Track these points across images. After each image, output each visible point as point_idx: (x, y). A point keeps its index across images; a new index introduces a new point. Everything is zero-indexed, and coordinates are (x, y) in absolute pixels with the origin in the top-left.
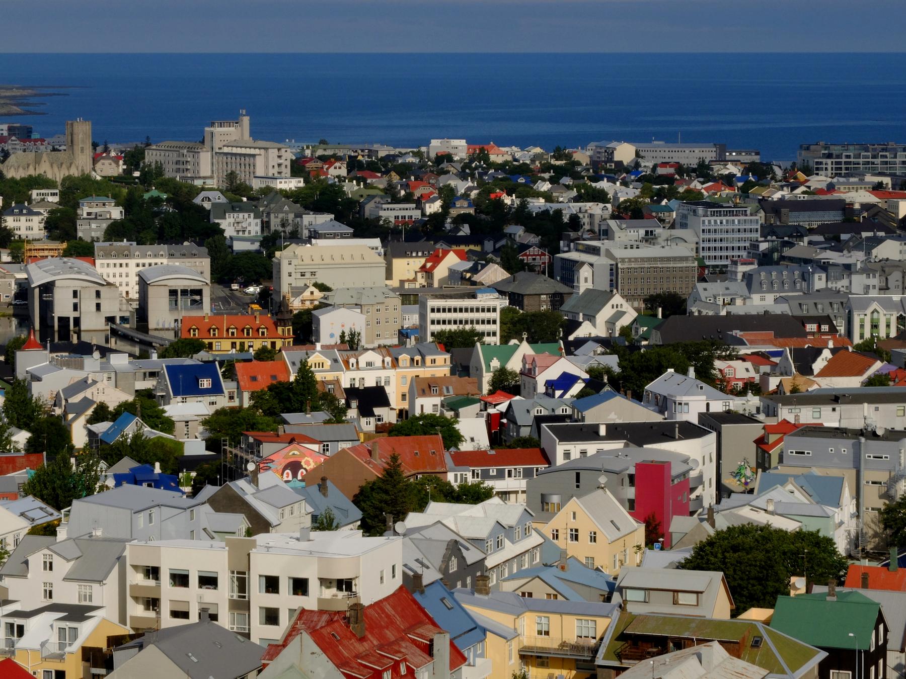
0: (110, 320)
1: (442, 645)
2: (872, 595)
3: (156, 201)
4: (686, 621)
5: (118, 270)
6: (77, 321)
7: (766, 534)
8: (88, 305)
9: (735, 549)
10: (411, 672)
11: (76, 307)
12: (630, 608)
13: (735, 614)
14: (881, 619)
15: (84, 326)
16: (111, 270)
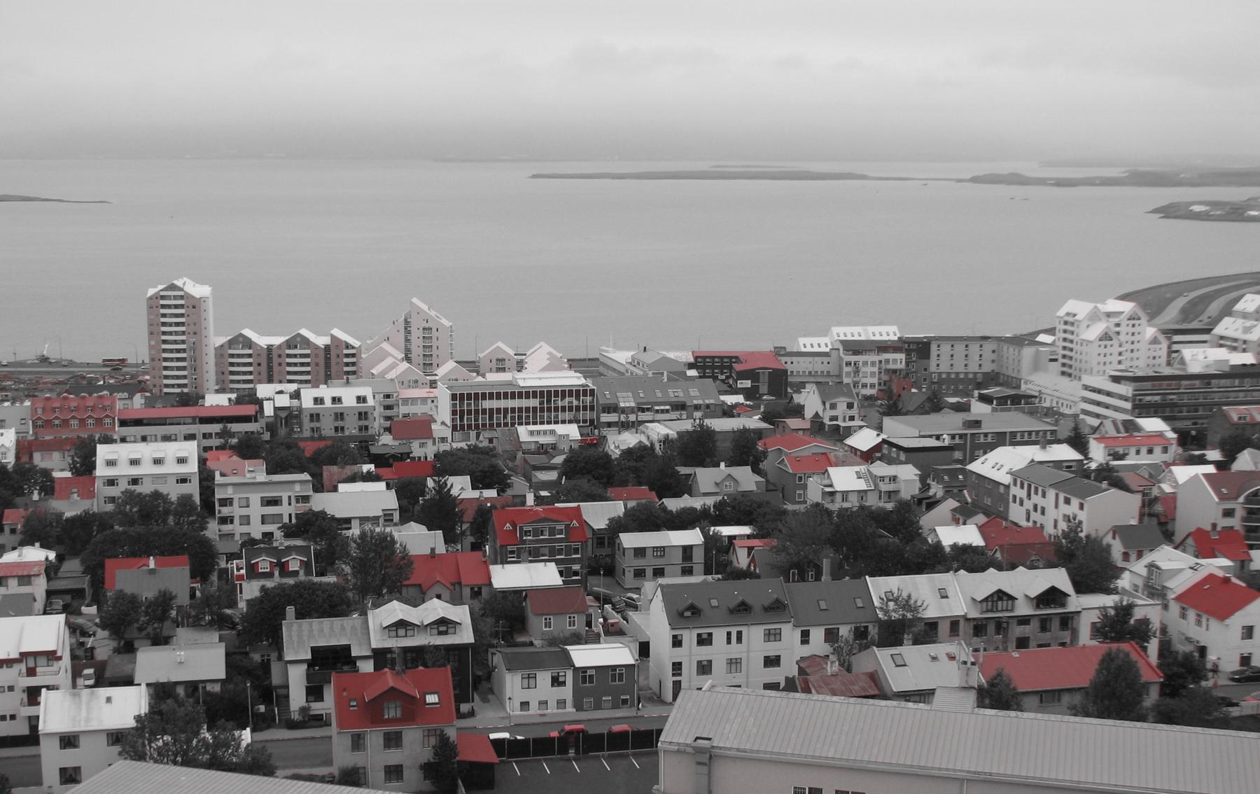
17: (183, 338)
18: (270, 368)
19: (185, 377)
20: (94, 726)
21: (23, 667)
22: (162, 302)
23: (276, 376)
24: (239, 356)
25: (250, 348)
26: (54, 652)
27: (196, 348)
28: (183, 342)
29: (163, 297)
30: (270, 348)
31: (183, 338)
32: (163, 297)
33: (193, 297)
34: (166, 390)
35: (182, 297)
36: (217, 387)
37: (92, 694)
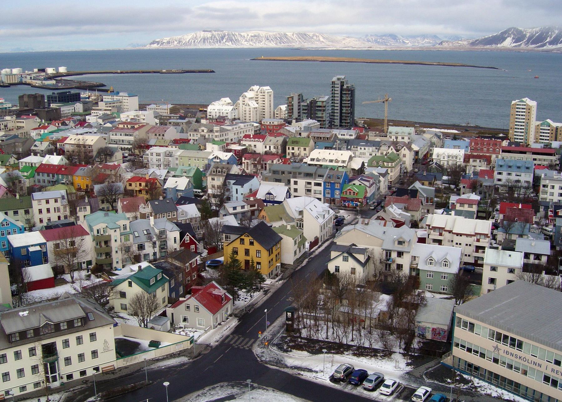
17: (524, 121)
18: (556, 135)
19: (523, 136)
20: (504, 264)
21: (475, 238)
22: (517, 106)
23: (558, 139)
24: (544, 129)
25: (549, 127)
26: (488, 234)
27: (528, 124)
28: (524, 122)
29: (518, 105)
30: (557, 128)
31: (524, 121)
32: (518, 105)
33: (530, 106)
34: (516, 140)
35: (525, 105)
36: (534, 141)
37: (504, 253)
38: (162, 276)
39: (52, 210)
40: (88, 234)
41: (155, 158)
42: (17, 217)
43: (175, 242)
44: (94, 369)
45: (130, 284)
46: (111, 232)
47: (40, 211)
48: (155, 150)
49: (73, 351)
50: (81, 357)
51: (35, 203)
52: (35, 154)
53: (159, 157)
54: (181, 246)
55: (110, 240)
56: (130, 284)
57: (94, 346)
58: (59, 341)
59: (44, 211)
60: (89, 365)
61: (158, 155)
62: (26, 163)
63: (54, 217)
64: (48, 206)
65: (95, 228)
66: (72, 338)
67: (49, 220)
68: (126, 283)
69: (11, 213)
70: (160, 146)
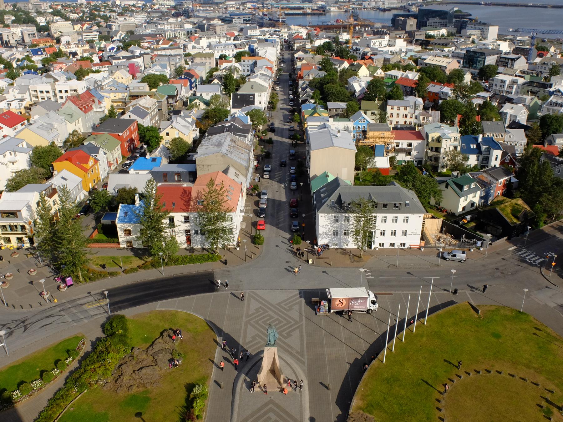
0: (16, 41)
1: (96, 100)
2: (174, 85)
3: (21, 15)
4: (141, 92)
5: (16, 30)
6: (9, 41)
7: (154, 75)
8: (11, 38)
9: (149, 78)
10: (91, 106)
11: (8, 38)
12: (131, 91)
13: (150, 90)
14: (176, 89)
15: (11, 42)
16: (14, 30)
38: (476, 185)
39: (401, 116)
40: (424, 140)
41: (499, 84)
42: (374, 117)
43: (496, 159)
44: (401, 244)
45: (447, 187)
46: (444, 140)
47: (392, 115)
48: (500, 77)
49: (389, 226)
50: (394, 233)
51: (389, 108)
52: (399, 69)
53: (503, 84)
54: (501, 164)
55: (440, 148)
56: (447, 187)
57: (405, 226)
58: (380, 216)
59: (395, 115)
60: (398, 240)
61: (503, 82)
62: (390, 75)
63: (402, 121)
64: (398, 112)
65: (431, 136)
66: (390, 217)
67: (397, 122)
68: (444, 185)
69: (369, 113)
70: (509, 75)
